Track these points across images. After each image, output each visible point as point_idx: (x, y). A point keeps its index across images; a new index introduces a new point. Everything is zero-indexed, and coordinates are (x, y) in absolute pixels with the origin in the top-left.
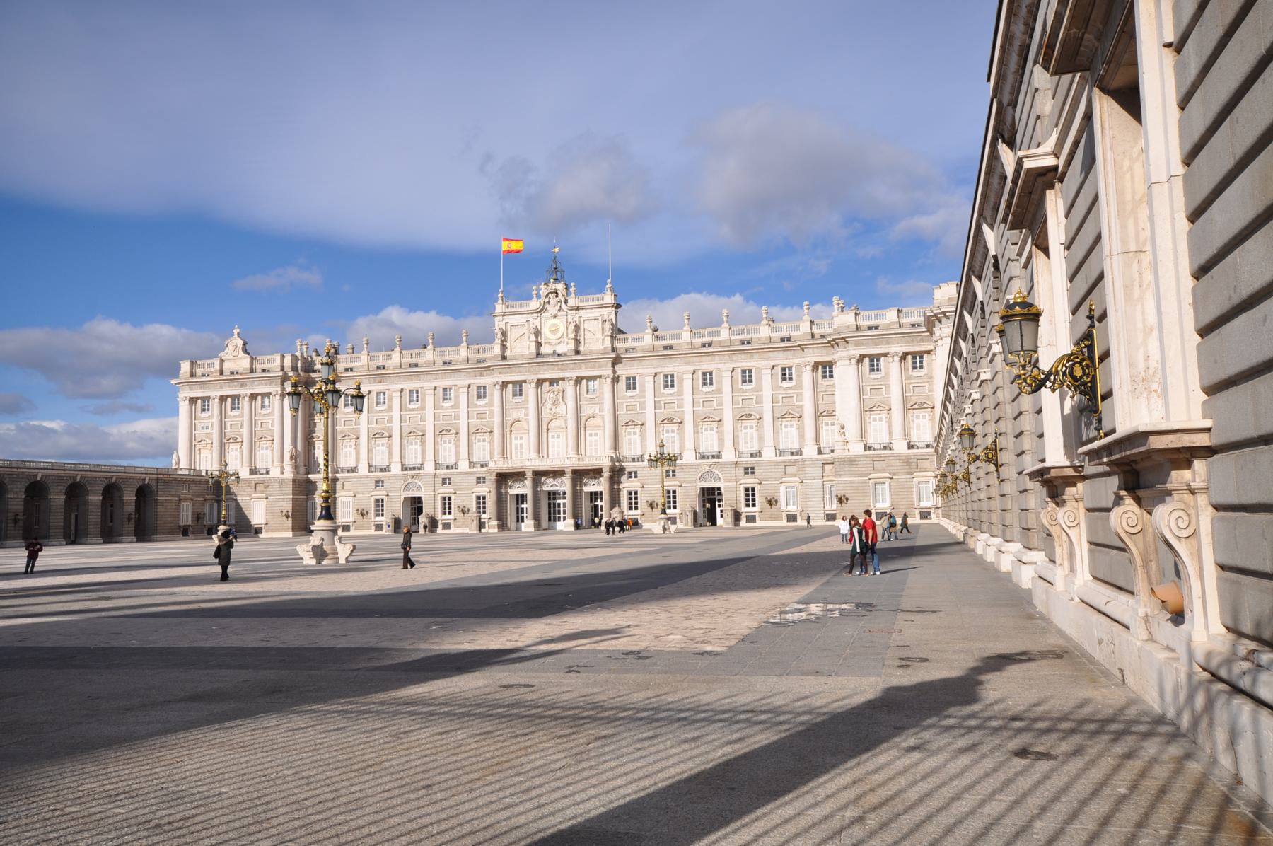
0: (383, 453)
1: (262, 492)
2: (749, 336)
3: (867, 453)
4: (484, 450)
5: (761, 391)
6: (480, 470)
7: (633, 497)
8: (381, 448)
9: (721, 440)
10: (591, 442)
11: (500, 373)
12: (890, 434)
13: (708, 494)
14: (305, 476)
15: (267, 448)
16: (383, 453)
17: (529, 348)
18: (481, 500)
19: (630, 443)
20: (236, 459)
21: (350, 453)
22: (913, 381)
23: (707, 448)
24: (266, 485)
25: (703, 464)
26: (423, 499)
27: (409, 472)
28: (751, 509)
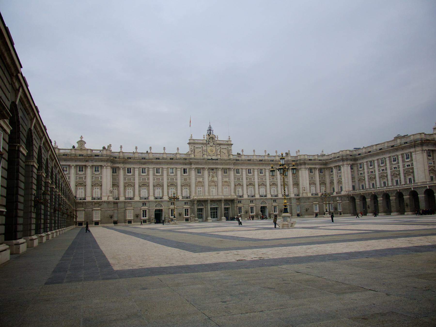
0: (145, 192)
1: (98, 207)
2: (273, 159)
3: (312, 196)
4: (187, 192)
5: (277, 176)
6: (186, 199)
7: (240, 209)
8: (144, 190)
9: (266, 191)
11: (194, 164)
15: (98, 189)
16: (145, 192)
17: (203, 157)
18: (186, 211)
19: (238, 191)
20: (82, 193)
21: (130, 192)
23: (262, 194)
24: (100, 204)
25: (262, 199)
26: (163, 210)
27: (158, 200)
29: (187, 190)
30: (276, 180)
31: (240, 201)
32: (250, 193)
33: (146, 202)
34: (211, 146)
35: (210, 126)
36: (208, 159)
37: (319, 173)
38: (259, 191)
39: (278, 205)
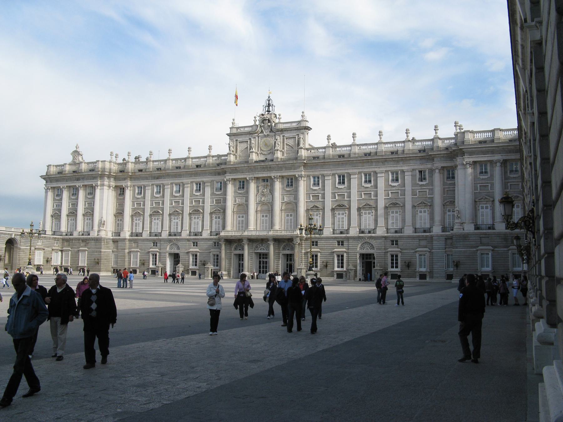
1: (85, 246)
4: (219, 224)
6: (215, 237)
9: (376, 221)
10: (288, 220)
11: (230, 173)
12: (493, 218)
13: (367, 258)
14: (112, 238)
16: (158, 224)
21: (139, 224)
22: (510, 181)
23: (366, 226)
25: (362, 237)
26: (180, 255)
28: (394, 269)
29: (219, 220)
30: (401, 196)
31: (317, 242)
32: (339, 225)
33: (156, 241)
34: (265, 136)
35: (269, 97)
36: (256, 162)
37: (506, 173)
38: (360, 220)
39: (401, 252)
